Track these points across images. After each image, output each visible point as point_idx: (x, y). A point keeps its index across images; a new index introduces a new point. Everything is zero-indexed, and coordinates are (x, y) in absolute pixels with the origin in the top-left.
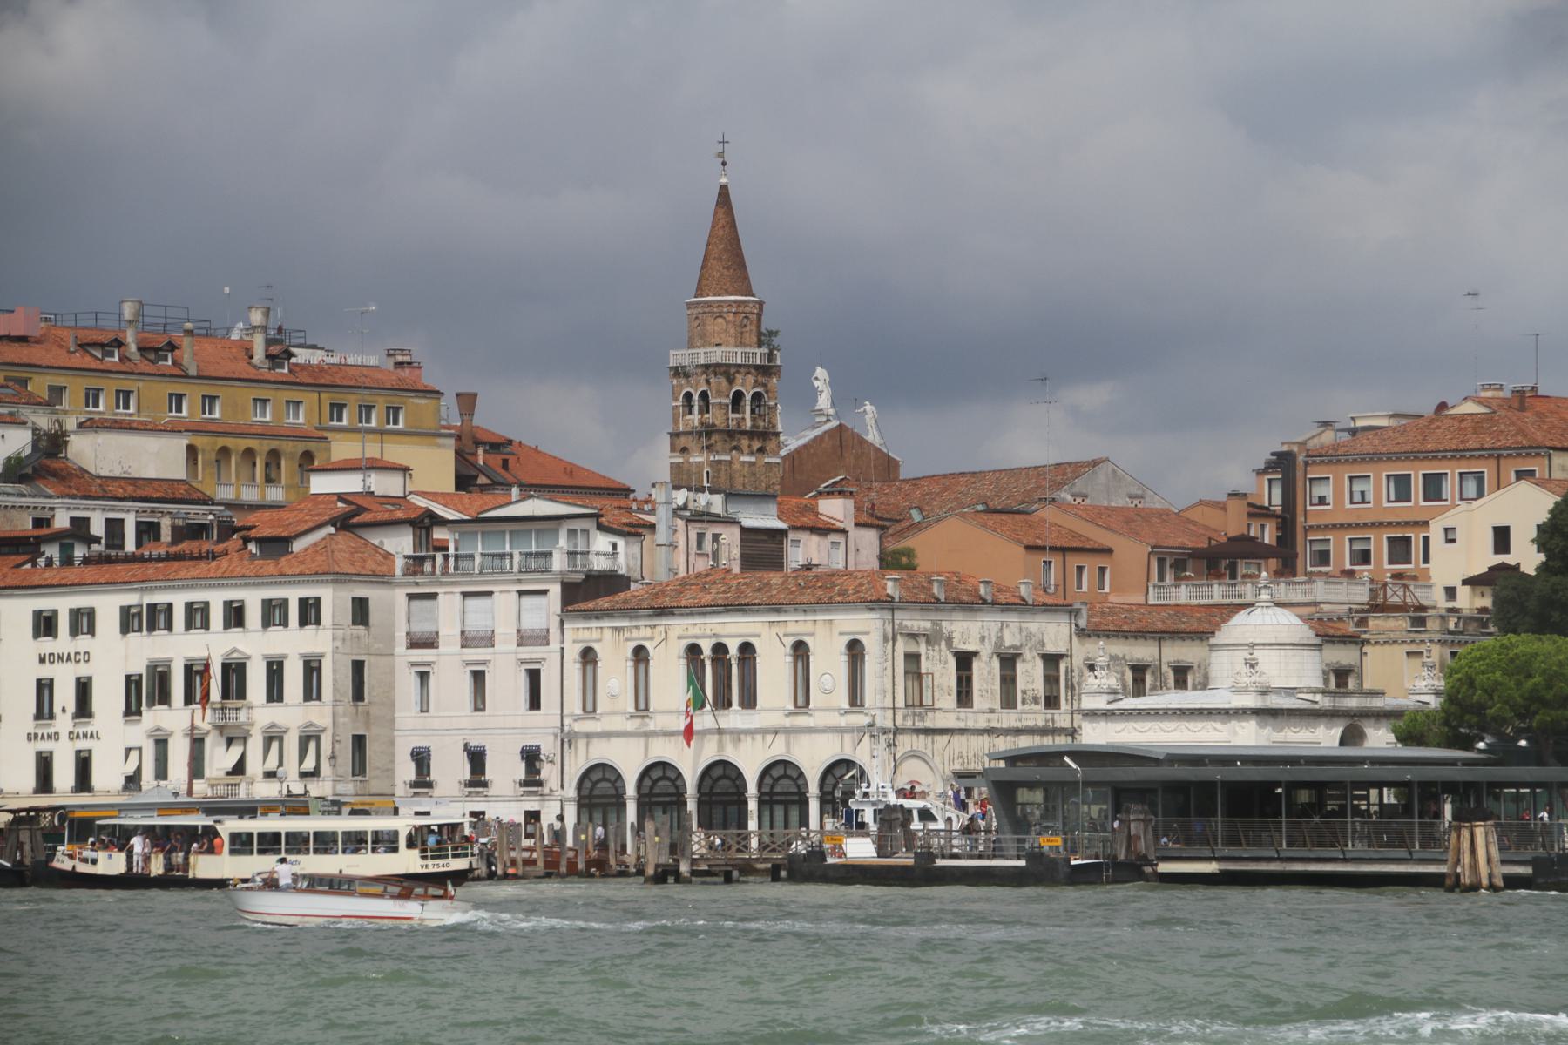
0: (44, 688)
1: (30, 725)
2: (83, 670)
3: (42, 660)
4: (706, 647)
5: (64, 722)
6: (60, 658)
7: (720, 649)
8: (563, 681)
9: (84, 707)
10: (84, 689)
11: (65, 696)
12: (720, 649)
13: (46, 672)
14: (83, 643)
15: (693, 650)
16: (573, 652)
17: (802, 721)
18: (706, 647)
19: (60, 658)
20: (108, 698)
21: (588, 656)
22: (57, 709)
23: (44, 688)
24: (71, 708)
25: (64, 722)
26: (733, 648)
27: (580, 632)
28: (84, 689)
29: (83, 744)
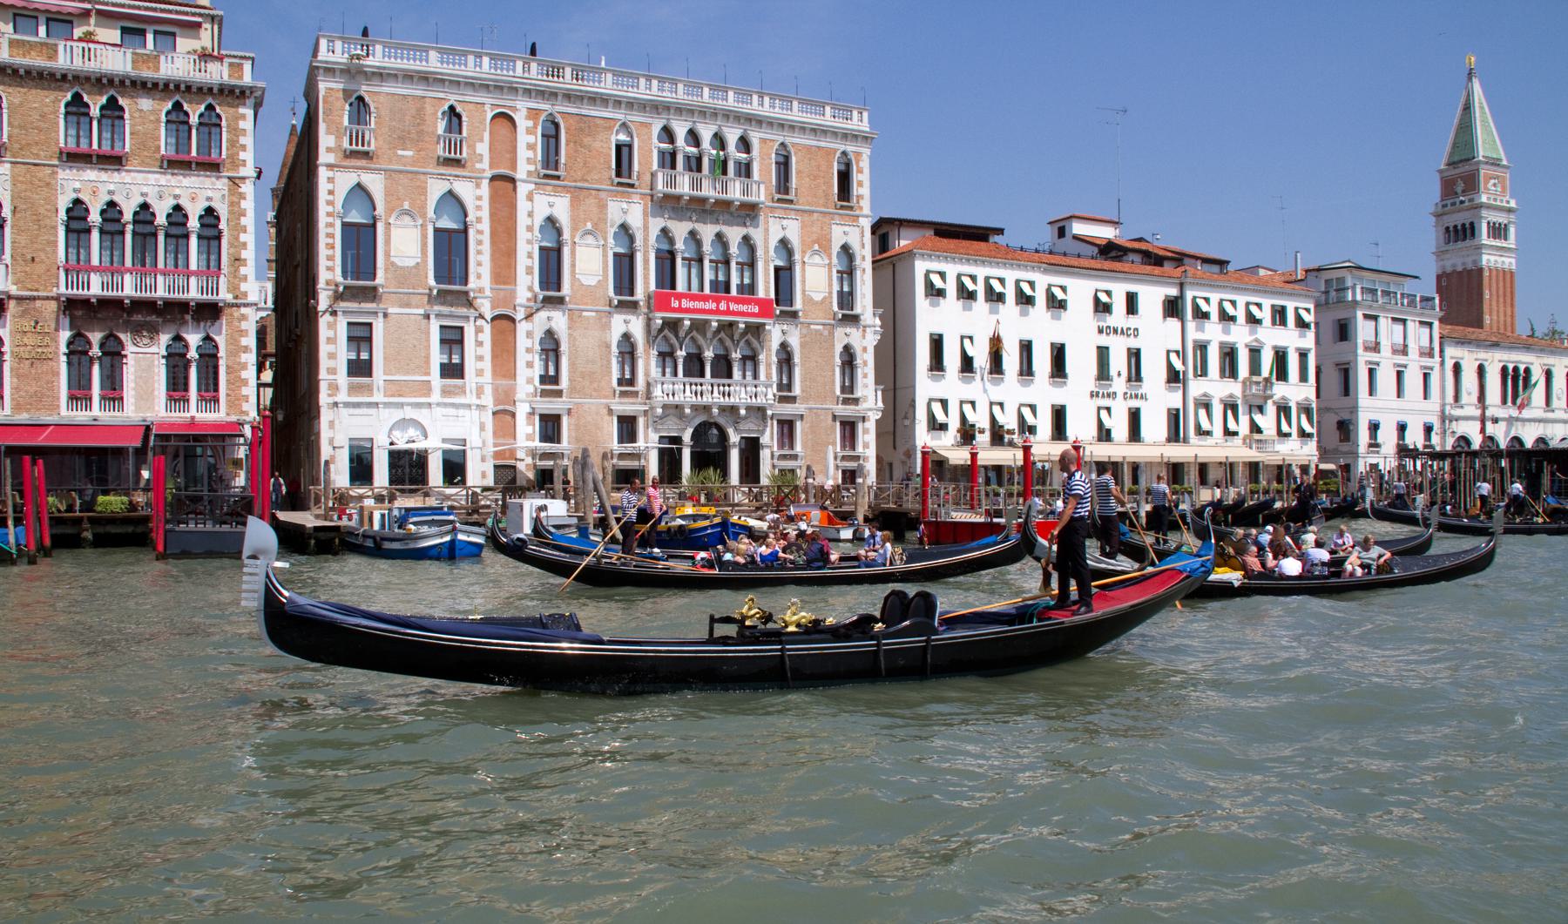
0: (1103, 353)
1: (1091, 384)
2: (1133, 343)
3: (1100, 331)
4: (1511, 367)
5: (1119, 385)
6: (1115, 331)
7: (1516, 369)
8: (1441, 381)
9: (1135, 375)
10: (1135, 355)
11: (1118, 363)
12: (1516, 369)
13: (1104, 340)
14: (1133, 322)
15: (1504, 370)
16: (1449, 364)
17: (1550, 415)
18: (1511, 367)
19: (1115, 331)
20: (1154, 370)
21: (1457, 368)
22: (1113, 372)
23: (1103, 353)
24: (1125, 374)
25: (1119, 385)
26: (1522, 368)
27: (1452, 352)
28: (1135, 355)
29: (1134, 403)
